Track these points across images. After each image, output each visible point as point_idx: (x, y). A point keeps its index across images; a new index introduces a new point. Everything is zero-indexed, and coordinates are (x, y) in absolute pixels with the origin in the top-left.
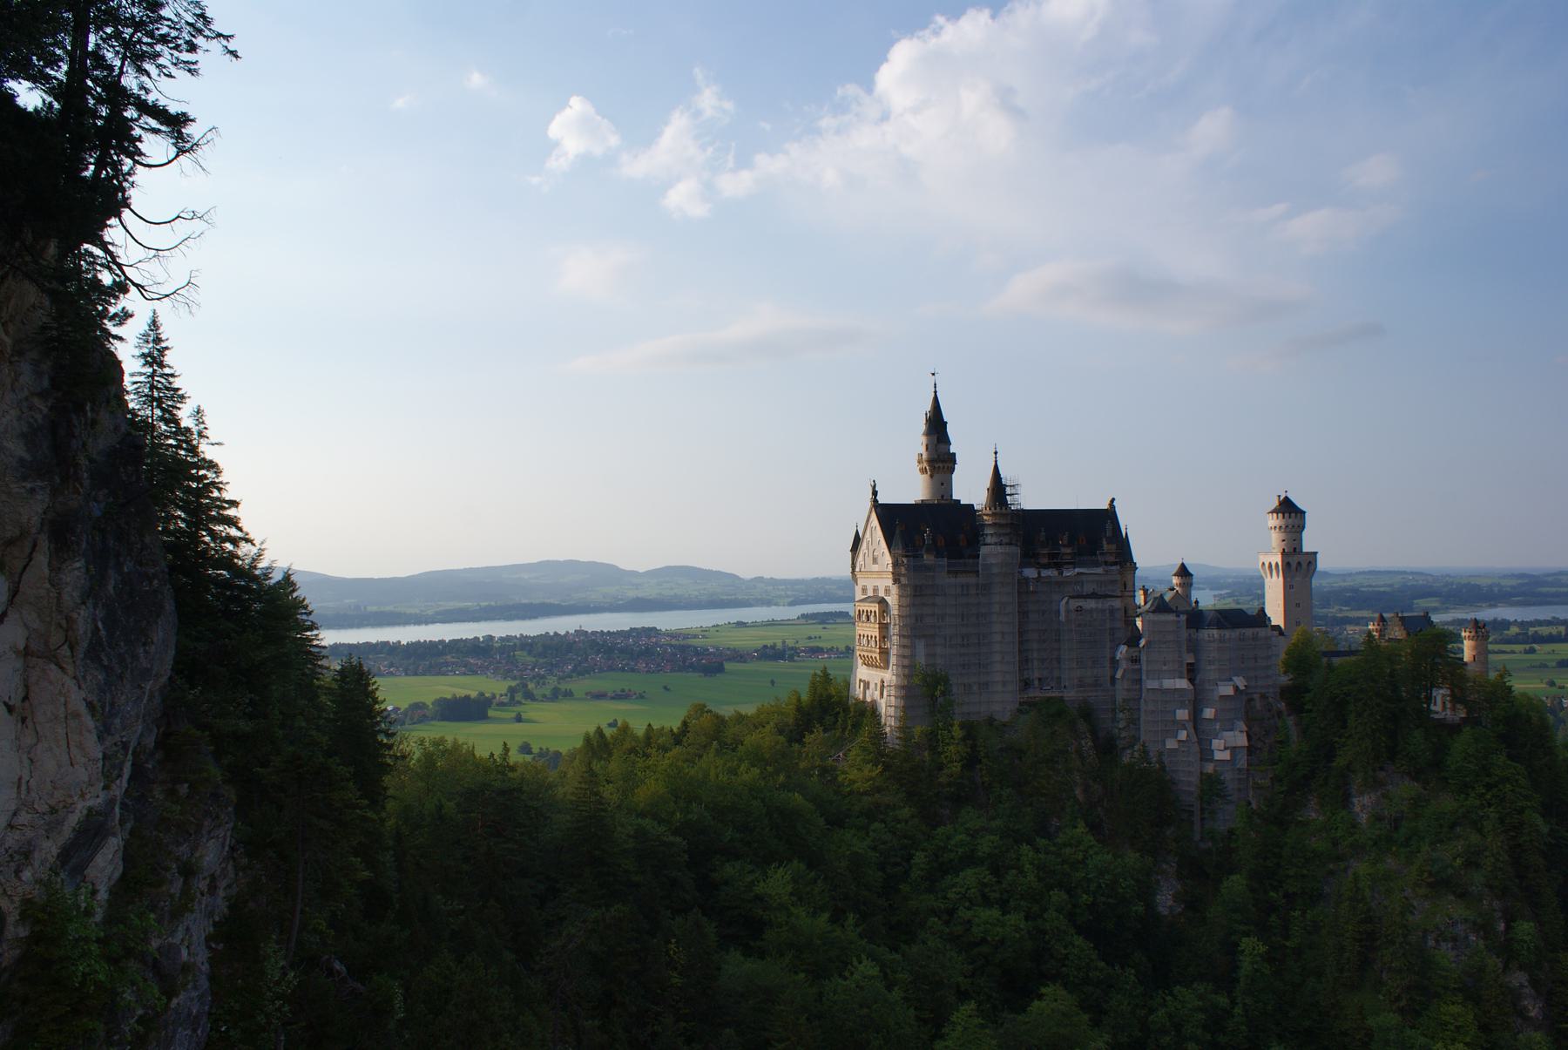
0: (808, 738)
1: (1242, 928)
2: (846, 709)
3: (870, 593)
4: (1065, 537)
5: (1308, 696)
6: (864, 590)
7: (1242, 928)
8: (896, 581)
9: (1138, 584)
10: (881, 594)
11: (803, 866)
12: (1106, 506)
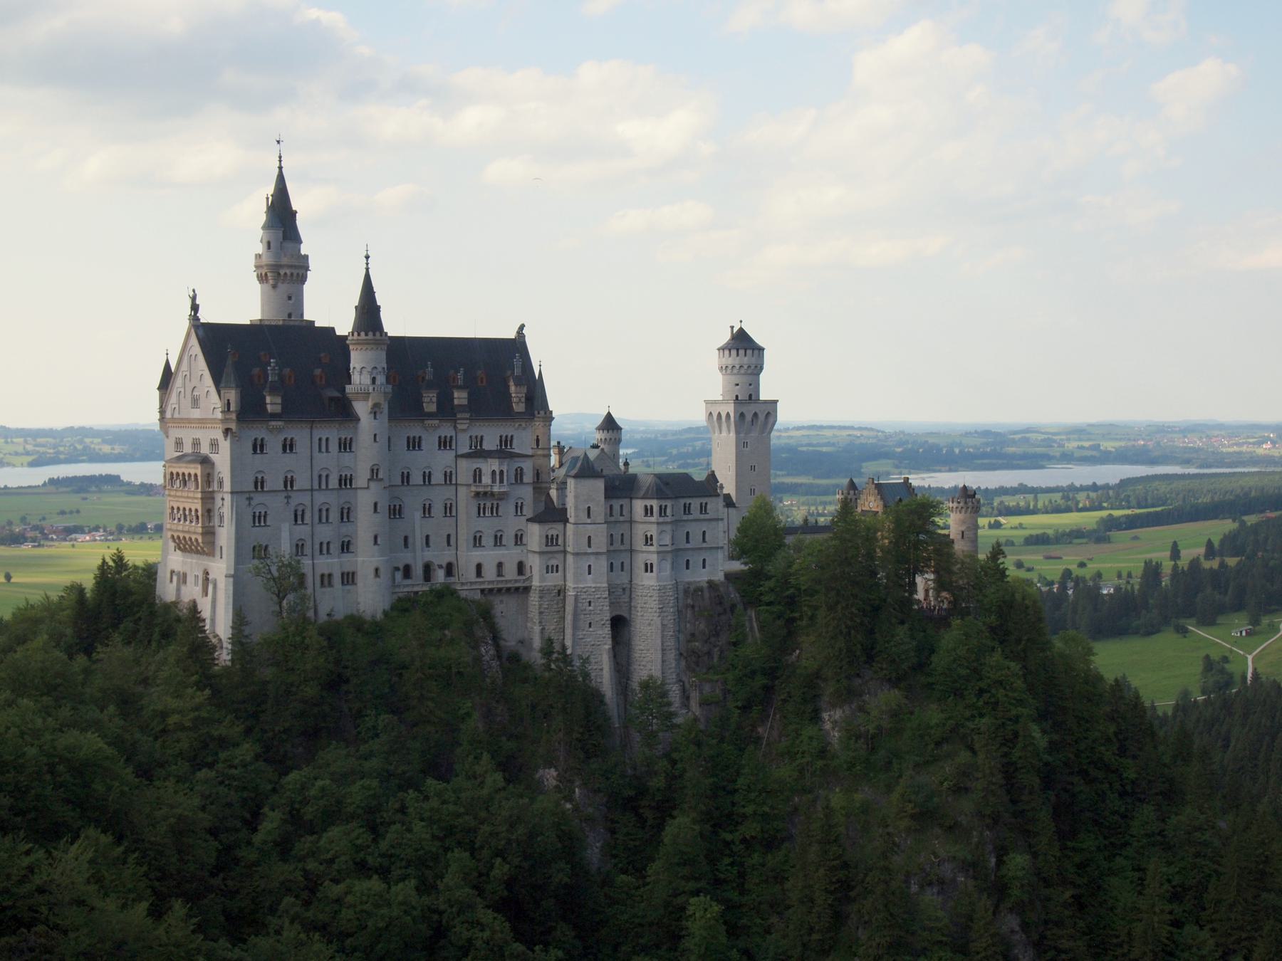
0: (101, 652)
1: (692, 885)
2: (152, 614)
3: (188, 449)
4: (460, 376)
5: (771, 583)
6: (179, 443)
7: (692, 885)
8: (227, 432)
9: (553, 443)
10: (205, 450)
11: (106, 839)
12: (511, 334)
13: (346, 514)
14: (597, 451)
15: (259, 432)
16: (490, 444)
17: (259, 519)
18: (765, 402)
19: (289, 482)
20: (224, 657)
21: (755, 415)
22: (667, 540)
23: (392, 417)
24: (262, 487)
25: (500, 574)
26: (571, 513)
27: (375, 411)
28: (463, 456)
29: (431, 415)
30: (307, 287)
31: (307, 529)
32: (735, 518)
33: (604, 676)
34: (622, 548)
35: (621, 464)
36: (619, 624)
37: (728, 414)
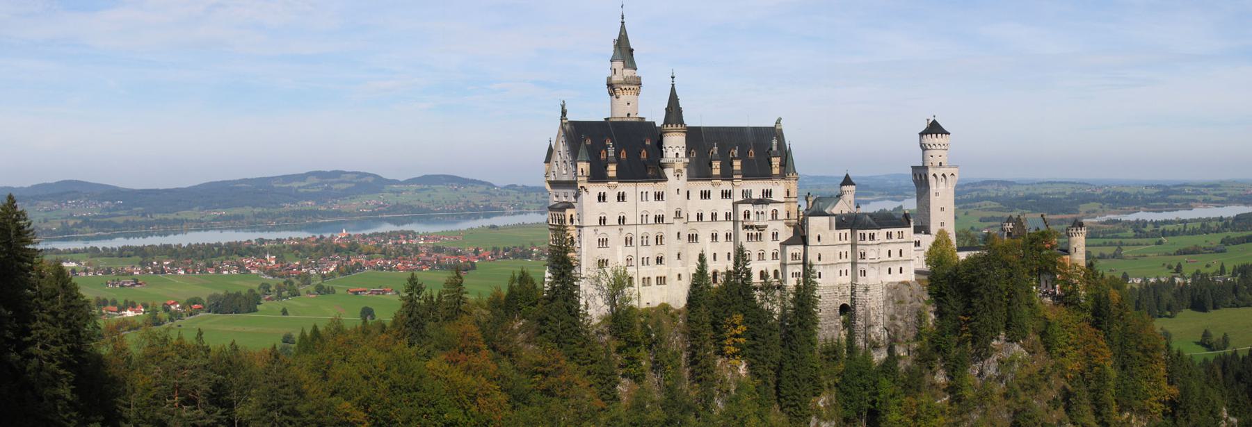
13: (659, 240)
16: (756, 195)
17: (603, 242)
19: (622, 220)
29: (717, 177)
31: (634, 249)
32: (927, 241)
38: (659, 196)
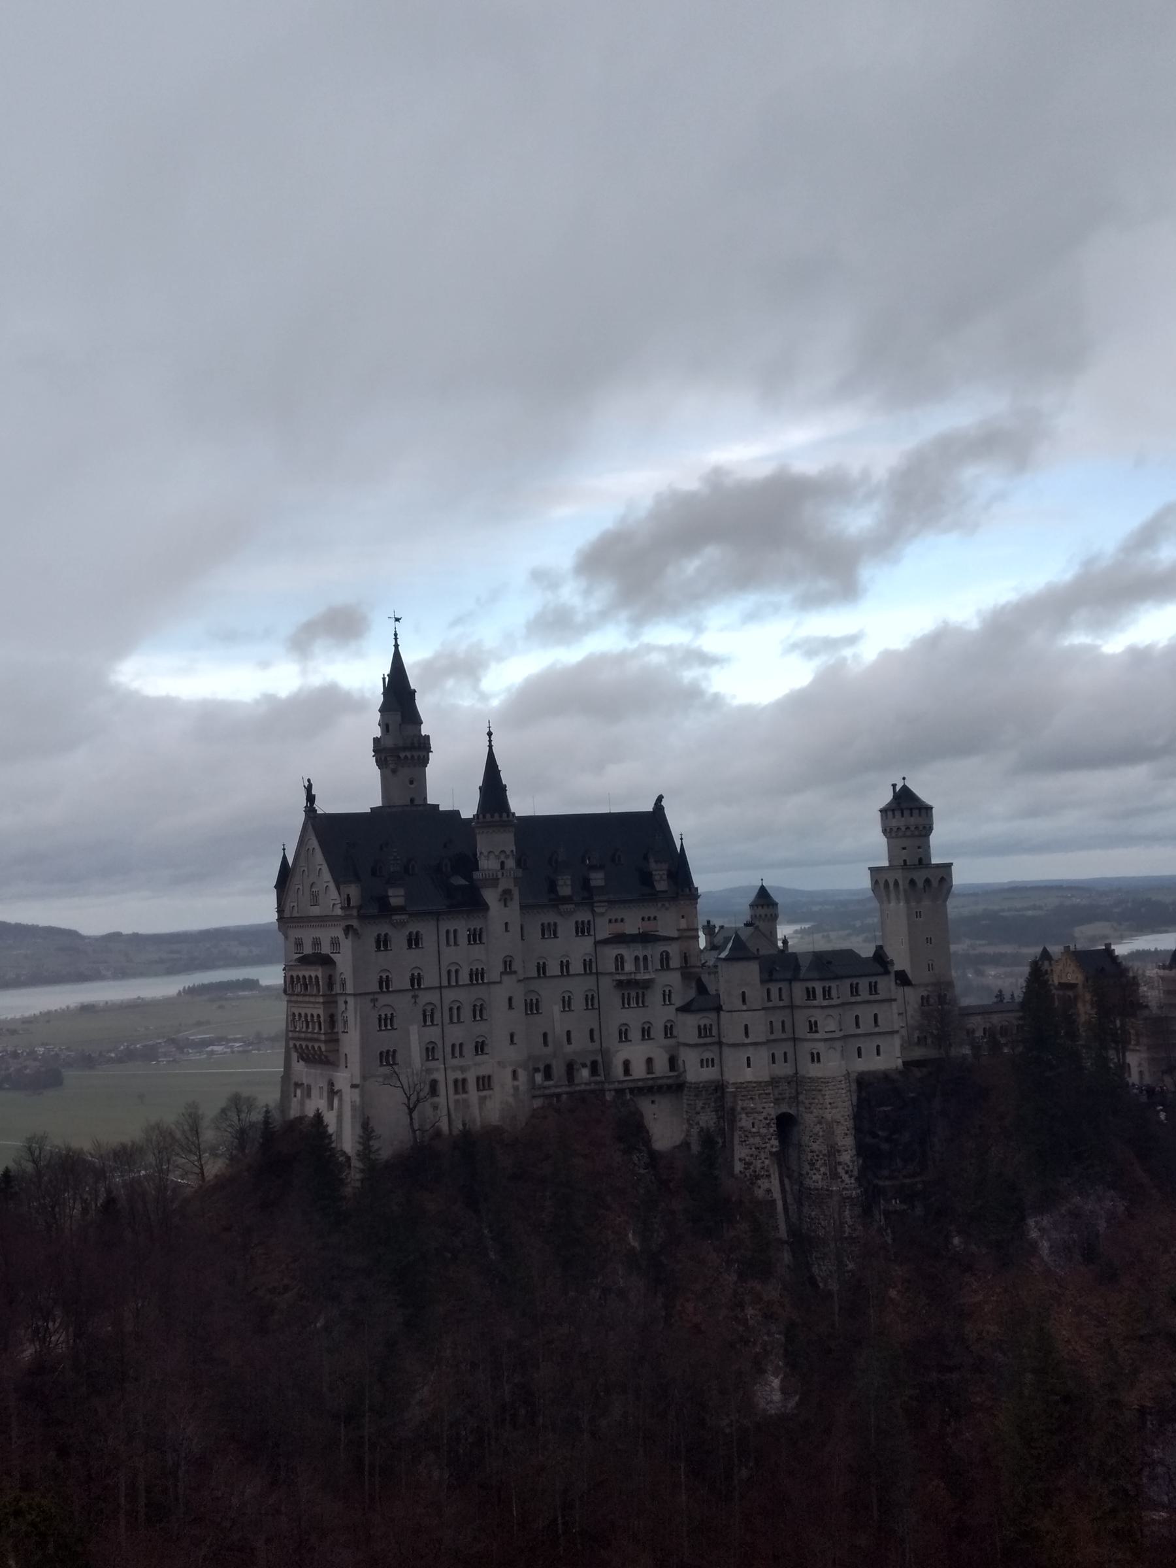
3: (308, 950)
6: (299, 943)
8: (348, 929)
10: (326, 949)
12: (649, 807)
13: (479, 1011)
14: (750, 929)
15: (384, 929)
17: (386, 1022)
18: (938, 866)
19: (416, 980)
20: (354, 1176)
21: (927, 881)
22: (832, 1025)
23: (523, 907)
24: (387, 987)
25: (650, 1070)
26: (724, 999)
27: (506, 897)
28: (606, 942)
29: (567, 900)
30: (429, 769)
32: (912, 996)
33: (771, 1186)
34: (784, 1036)
35: (780, 944)
36: (785, 1124)
37: (896, 883)
38: (475, 937)
